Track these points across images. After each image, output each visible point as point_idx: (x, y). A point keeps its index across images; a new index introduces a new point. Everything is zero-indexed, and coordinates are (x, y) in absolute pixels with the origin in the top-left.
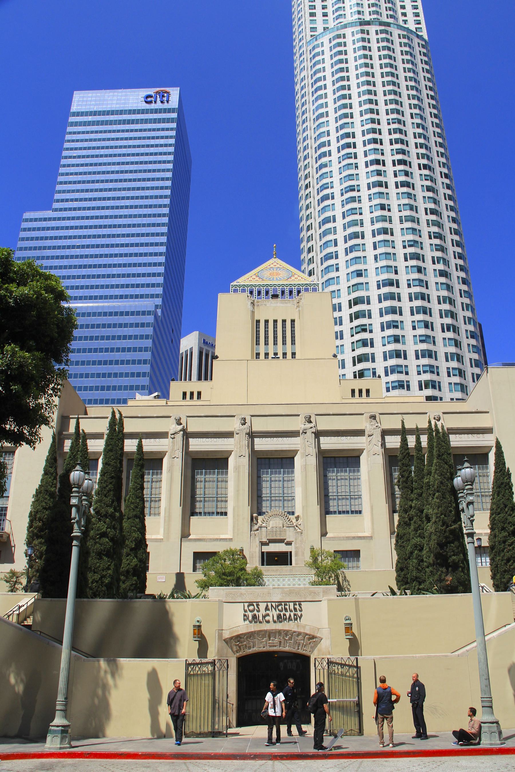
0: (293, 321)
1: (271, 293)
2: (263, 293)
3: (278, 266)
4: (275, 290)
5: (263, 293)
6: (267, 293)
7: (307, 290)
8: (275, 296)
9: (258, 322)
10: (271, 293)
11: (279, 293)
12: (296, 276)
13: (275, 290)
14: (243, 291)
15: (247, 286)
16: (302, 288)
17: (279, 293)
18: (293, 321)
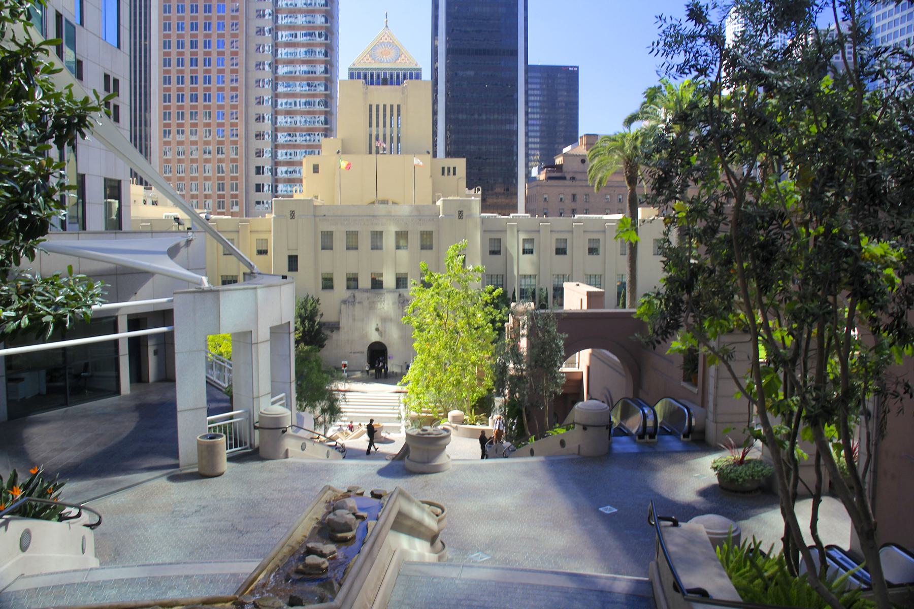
0: (399, 106)
1: (382, 77)
2: (375, 77)
3: (388, 39)
4: (385, 74)
5: (375, 77)
6: (378, 76)
7: (411, 78)
8: (385, 82)
9: (371, 106)
10: (382, 77)
11: (388, 77)
12: (403, 56)
13: (385, 74)
14: (359, 77)
15: (362, 69)
16: (408, 73)
17: (388, 77)
18: (399, 106)
